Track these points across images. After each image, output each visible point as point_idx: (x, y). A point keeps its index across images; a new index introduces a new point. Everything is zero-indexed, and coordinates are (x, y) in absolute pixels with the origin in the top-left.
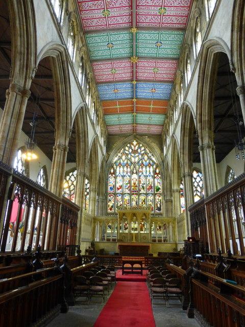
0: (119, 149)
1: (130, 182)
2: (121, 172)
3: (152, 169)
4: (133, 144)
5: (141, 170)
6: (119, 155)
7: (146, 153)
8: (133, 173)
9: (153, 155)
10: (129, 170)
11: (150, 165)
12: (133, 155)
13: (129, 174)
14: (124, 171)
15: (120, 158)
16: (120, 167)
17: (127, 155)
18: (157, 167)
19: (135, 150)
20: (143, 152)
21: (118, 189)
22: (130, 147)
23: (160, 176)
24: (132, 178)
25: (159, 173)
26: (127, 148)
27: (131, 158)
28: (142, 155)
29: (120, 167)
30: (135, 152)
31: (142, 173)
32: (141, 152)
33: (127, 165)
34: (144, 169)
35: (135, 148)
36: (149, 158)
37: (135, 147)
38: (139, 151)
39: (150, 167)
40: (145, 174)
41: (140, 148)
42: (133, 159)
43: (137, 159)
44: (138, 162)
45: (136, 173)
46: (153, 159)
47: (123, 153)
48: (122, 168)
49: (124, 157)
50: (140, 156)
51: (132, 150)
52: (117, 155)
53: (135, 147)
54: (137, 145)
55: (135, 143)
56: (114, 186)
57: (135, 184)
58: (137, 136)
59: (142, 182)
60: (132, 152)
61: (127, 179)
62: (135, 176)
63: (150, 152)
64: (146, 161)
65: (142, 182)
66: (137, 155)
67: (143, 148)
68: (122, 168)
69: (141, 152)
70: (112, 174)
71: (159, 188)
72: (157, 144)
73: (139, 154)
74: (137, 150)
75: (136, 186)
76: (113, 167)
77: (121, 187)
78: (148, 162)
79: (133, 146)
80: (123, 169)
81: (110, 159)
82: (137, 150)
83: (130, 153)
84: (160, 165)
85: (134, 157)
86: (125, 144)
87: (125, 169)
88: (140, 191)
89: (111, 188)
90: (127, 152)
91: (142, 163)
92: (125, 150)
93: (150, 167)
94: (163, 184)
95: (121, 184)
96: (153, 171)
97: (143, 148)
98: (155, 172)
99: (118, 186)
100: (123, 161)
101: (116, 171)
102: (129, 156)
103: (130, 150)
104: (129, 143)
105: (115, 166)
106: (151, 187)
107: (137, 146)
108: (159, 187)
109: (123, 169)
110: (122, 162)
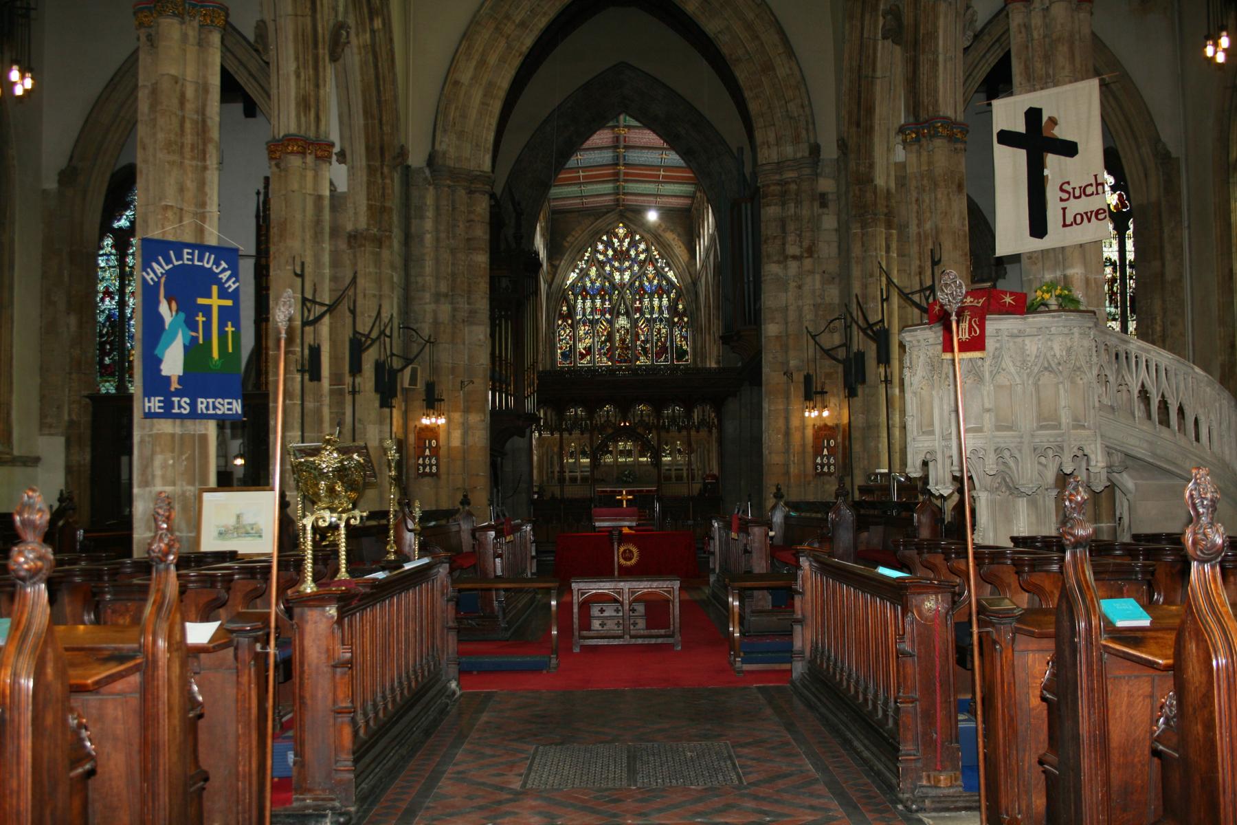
0: (582, 251)
1: (610, 337)
2: (588, 310)
3: (665, 301)
4: (616, 236)
5: (638, 304)
6: (582, 265)
7: (650, 260)
8: (619, 314)
9: (668, 264)
10: (607, 305)
11: (660, 291)
12: (616, 264)
13: (608, 316)
14: (594, 309)
15: (584, 274)
16: (584, 299)
17: (602, 265)
18: (679, 296)
19: (622, 251)
20: (642, 257)
21: (583, 356)
22: (609, 244)
23: (686, 319)
24: (617, 326)
25: (684, 314)
26: (601, 247)
27: (611, 274)
28: (642, 264)
29: (584, 299)
30: (621, 255)
31: (642, 314)
32: (637, 255)
33: (602, 293)
34: (646, 301)
35: (621, 245)
36: (660, 273)
37: (621, 241)
38: (633, 253)
39: (660, 298)
40: (648, 316)
41: (633, 244)
42: (617, 276)
43: (627, 276)
44: (632, 285)
45: (627, 314)
46: (671, 274)
47: (592, 261)
48: (588, 303)
49: (593, 272)
50: (636, 268)
51: (615, 250)
52: (576, 266)
53: (621, 241)
54: (626, 236)
55: (621, 231)
56: (573, 348)
57: (623, 341)
58: (629, 214)
59: (642, 338)
60: (615, 258)
61: (603, 327)
62: (622, 321)
63: (662, 257)
64: (651, 282)
65: (642, 338)
66: (627, 264)
67: (642, 246)
68: (588, 303)
69: (637, 255)
70: (564, 318)
71: (686, 352)
72: (679, 235)
73: (634, 261)
74: (628, 250)
75: (628, 348)
76: (566, 300)
77: (589, 350)
78: (656, 282)
79: (615, 240)
80: (593, 302)
81: (557, 280)
82: (628, 250)
83: (609, 261)
84: (688, 291)
85: (618, 269)
86: (595, 237)
87: (598, 302)
88: (638, 359)
89: (562, 354)
90: (601, 257)
91: (642, 286)
92: (596, 251)
93: (660, 298)
94: (694, 341)
95: (588, 342)
96: (669, 308)
97: (642, 246)
98: (673, 308)
99: (581, 347)
100: (593, 283)
101: (575, 307)
102: (608, 268)
103: (610, 253)
104: (607, 233)
105: (572, 297)
106: (664, 349)
107: (627, 240)
108: (685, 347)
109: (593, 302)
110: (589, 284)
